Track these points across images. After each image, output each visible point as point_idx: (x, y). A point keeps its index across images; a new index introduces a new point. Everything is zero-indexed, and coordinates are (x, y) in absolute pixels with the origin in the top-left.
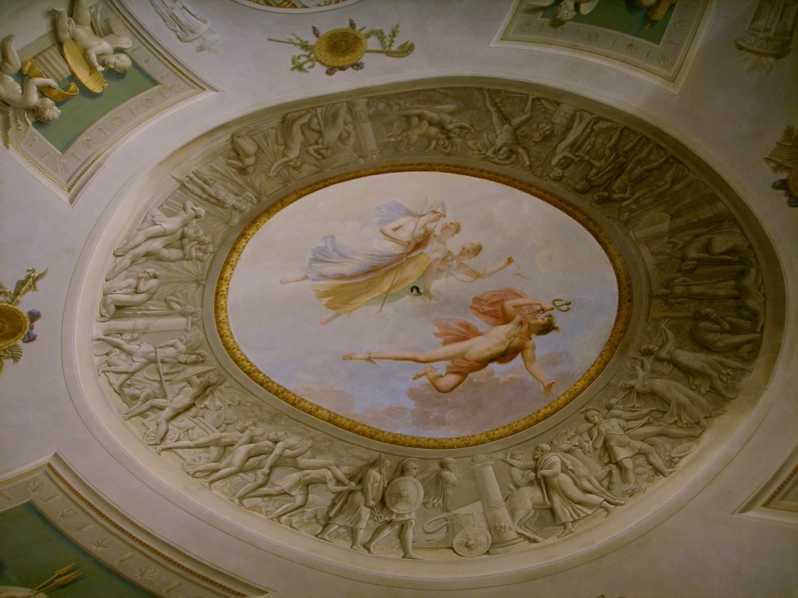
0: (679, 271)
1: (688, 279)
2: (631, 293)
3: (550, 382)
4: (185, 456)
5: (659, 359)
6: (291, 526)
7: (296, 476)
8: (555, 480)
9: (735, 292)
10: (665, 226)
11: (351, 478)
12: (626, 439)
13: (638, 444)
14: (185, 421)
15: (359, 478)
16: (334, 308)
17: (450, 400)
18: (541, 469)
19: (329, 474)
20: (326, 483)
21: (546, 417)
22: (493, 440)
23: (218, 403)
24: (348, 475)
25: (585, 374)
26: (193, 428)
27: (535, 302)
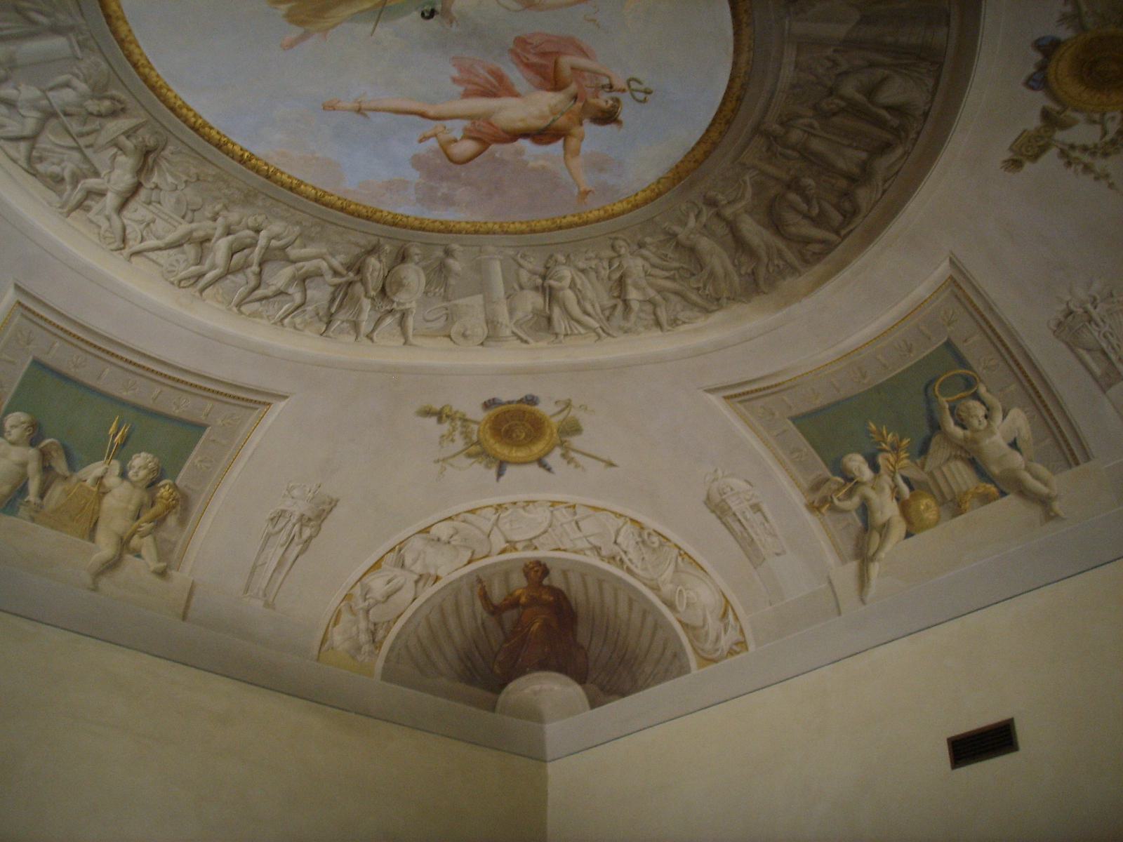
0: (815, 107)
1: (816, 125)
2: (735, 111)
3: (588, 189)
4: (162, 261)
5: (718, 215)
6: (295, 328)
7: (288, 271)
8: (561, 293)
9: (856, 170)
10: (841, 31)
11: (349, 268)
12: (643, 283)
13: (652, 293)
14: (137, 211)
15: (357, 267)
16: (301, 23)
17: (463, 174)
18: (550, 279)
19: (324, 265)
20: (322, 275)
21: (570, 226)
22: (506, 233)
23: (170, 179)
24: (345, 264)
25: (631, 196)
26: (154, 221)
27: (603, 71)
